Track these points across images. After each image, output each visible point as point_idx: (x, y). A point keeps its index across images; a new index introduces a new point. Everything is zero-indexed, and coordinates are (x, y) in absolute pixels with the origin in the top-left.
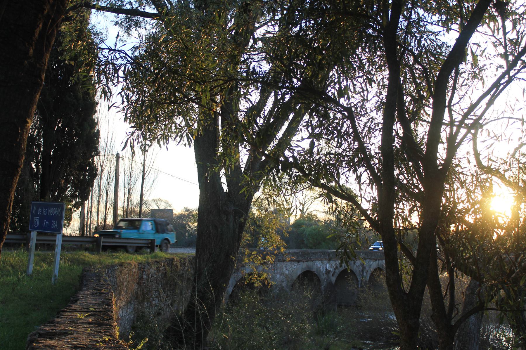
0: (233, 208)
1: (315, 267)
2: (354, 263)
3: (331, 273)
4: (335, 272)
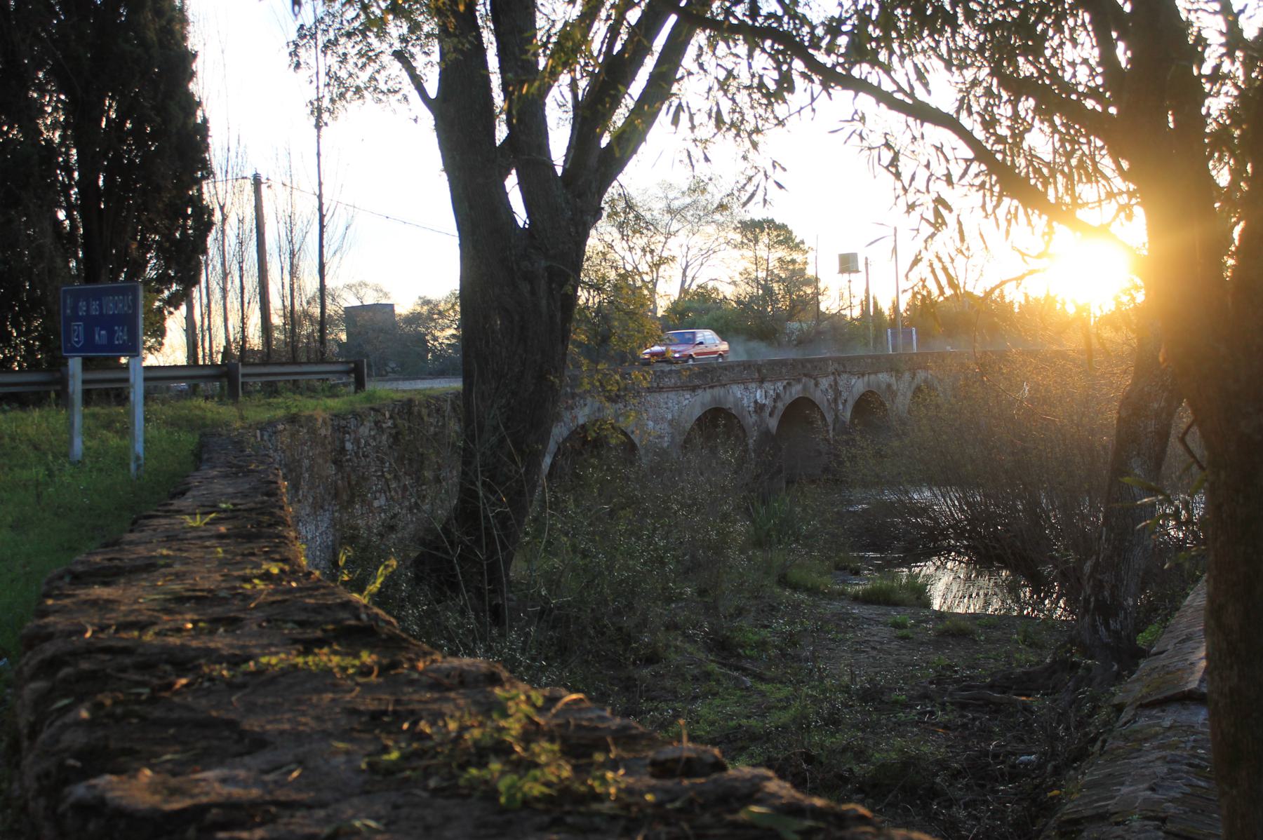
1: (731, 399)
2: (817, 385)
3: (768, 411)
4: (775, 407)
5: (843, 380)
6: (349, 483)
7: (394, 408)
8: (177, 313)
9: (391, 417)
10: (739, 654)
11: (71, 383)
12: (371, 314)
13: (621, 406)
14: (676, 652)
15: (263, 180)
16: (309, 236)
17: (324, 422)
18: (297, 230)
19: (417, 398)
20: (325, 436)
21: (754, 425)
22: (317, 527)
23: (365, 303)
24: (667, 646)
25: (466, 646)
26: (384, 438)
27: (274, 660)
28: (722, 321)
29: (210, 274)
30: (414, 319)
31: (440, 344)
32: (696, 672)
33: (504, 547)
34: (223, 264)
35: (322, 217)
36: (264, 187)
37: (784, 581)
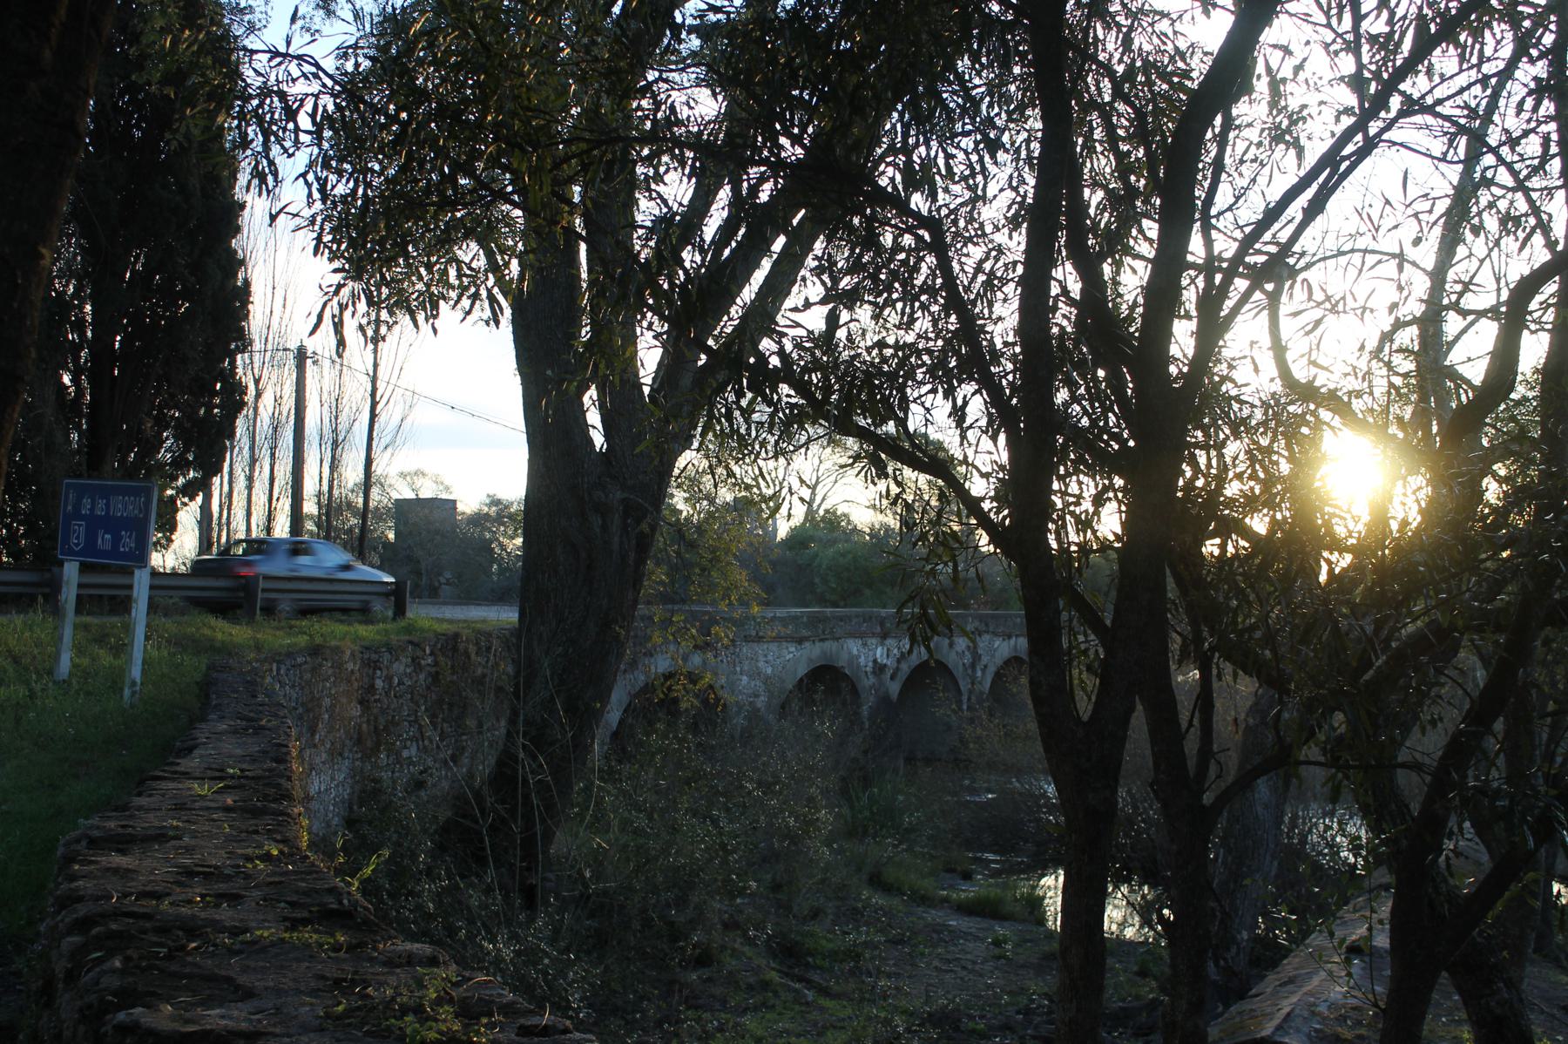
0: (619, 495)
1: (845, 656)
2: (951, 645)
3: (889, 673)
4: (898, 669)
5: (983, 642)
6: (376, 728)
7: (436, 643)
8: (192, 504)
9: (432, 654)
10: (807, 964)
11: (64, 589)
12: (427, 511)
13: (710, 655)
14: (732, 956)
15: (309, 354)
16: (357, 423)
17: (353, 654)
18: (343, 418)
19: (465, 633)
20: (352, 671)
21: (871, 688)
22: (333, 779)
23: (421, 496)
24: (723, 948)
25: (489, 931)
26: (422, 677)
27: (266, 934)
28: (850, 556)
29: (237, 460)
30: (478, 519)
31: (509, 554)
32: (751, 980)
33: (543, 821)
34: (252, 448)
35: (374, 405)
36: (309, 361)
37: (877, 881)
